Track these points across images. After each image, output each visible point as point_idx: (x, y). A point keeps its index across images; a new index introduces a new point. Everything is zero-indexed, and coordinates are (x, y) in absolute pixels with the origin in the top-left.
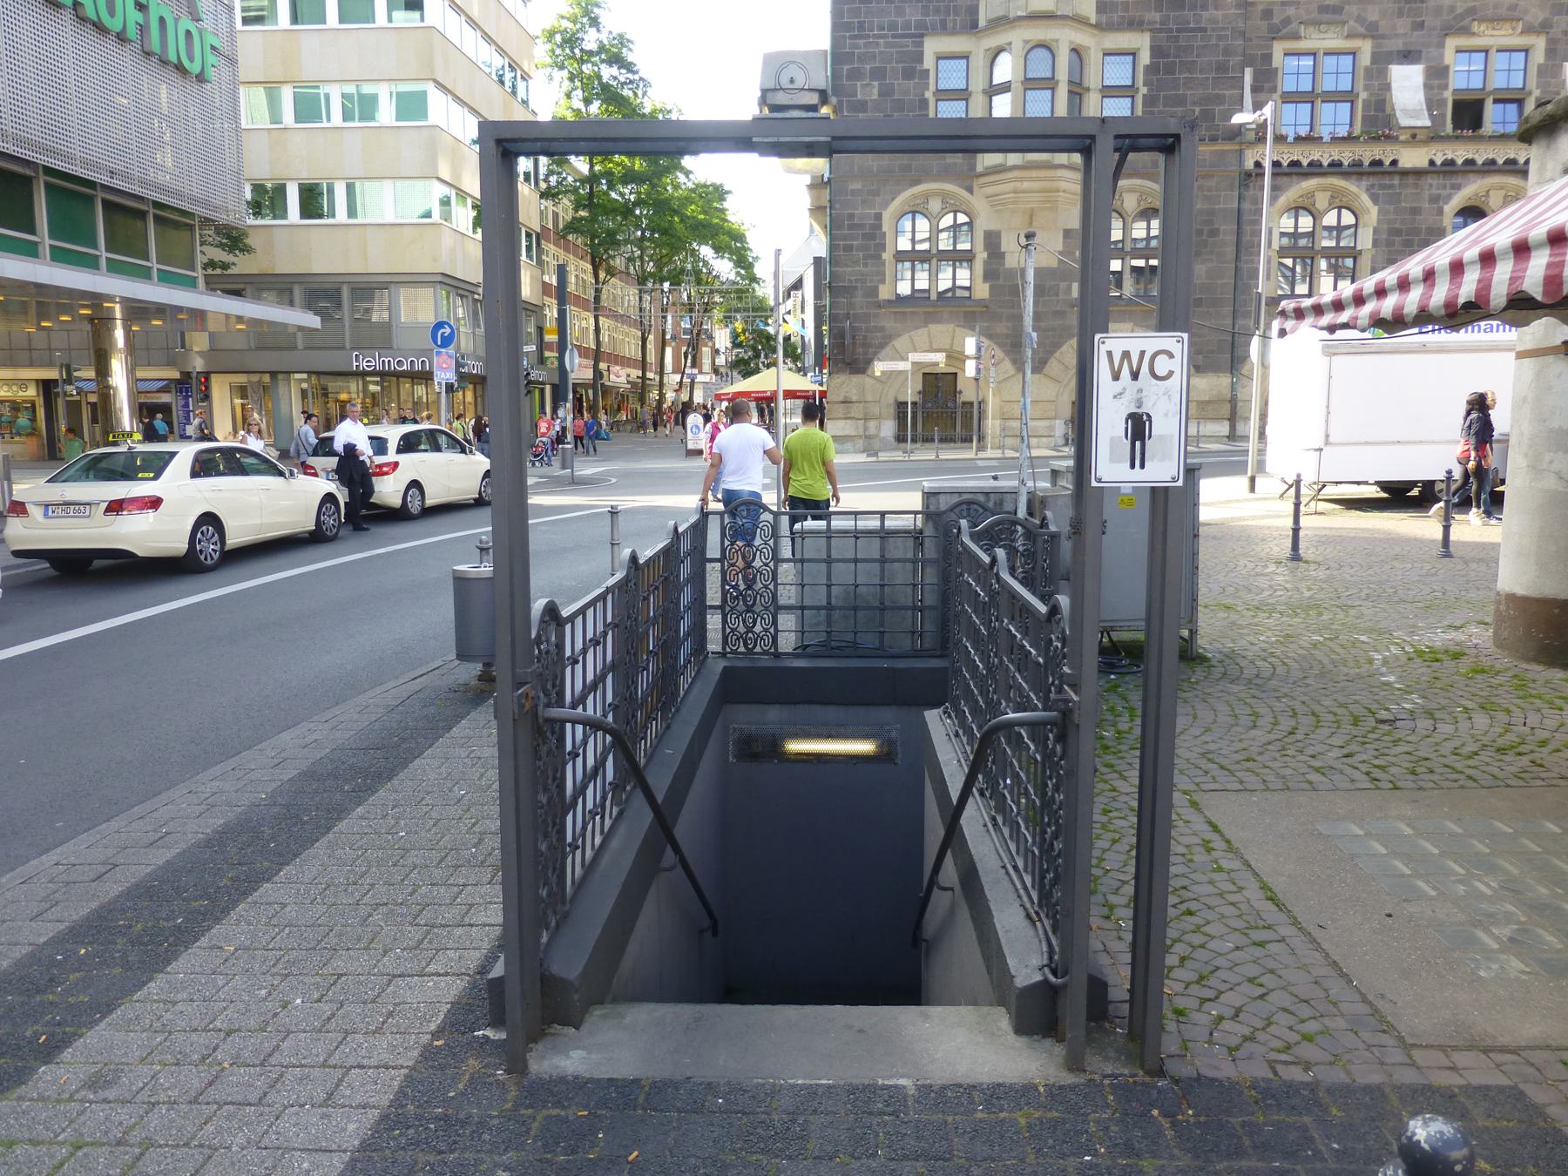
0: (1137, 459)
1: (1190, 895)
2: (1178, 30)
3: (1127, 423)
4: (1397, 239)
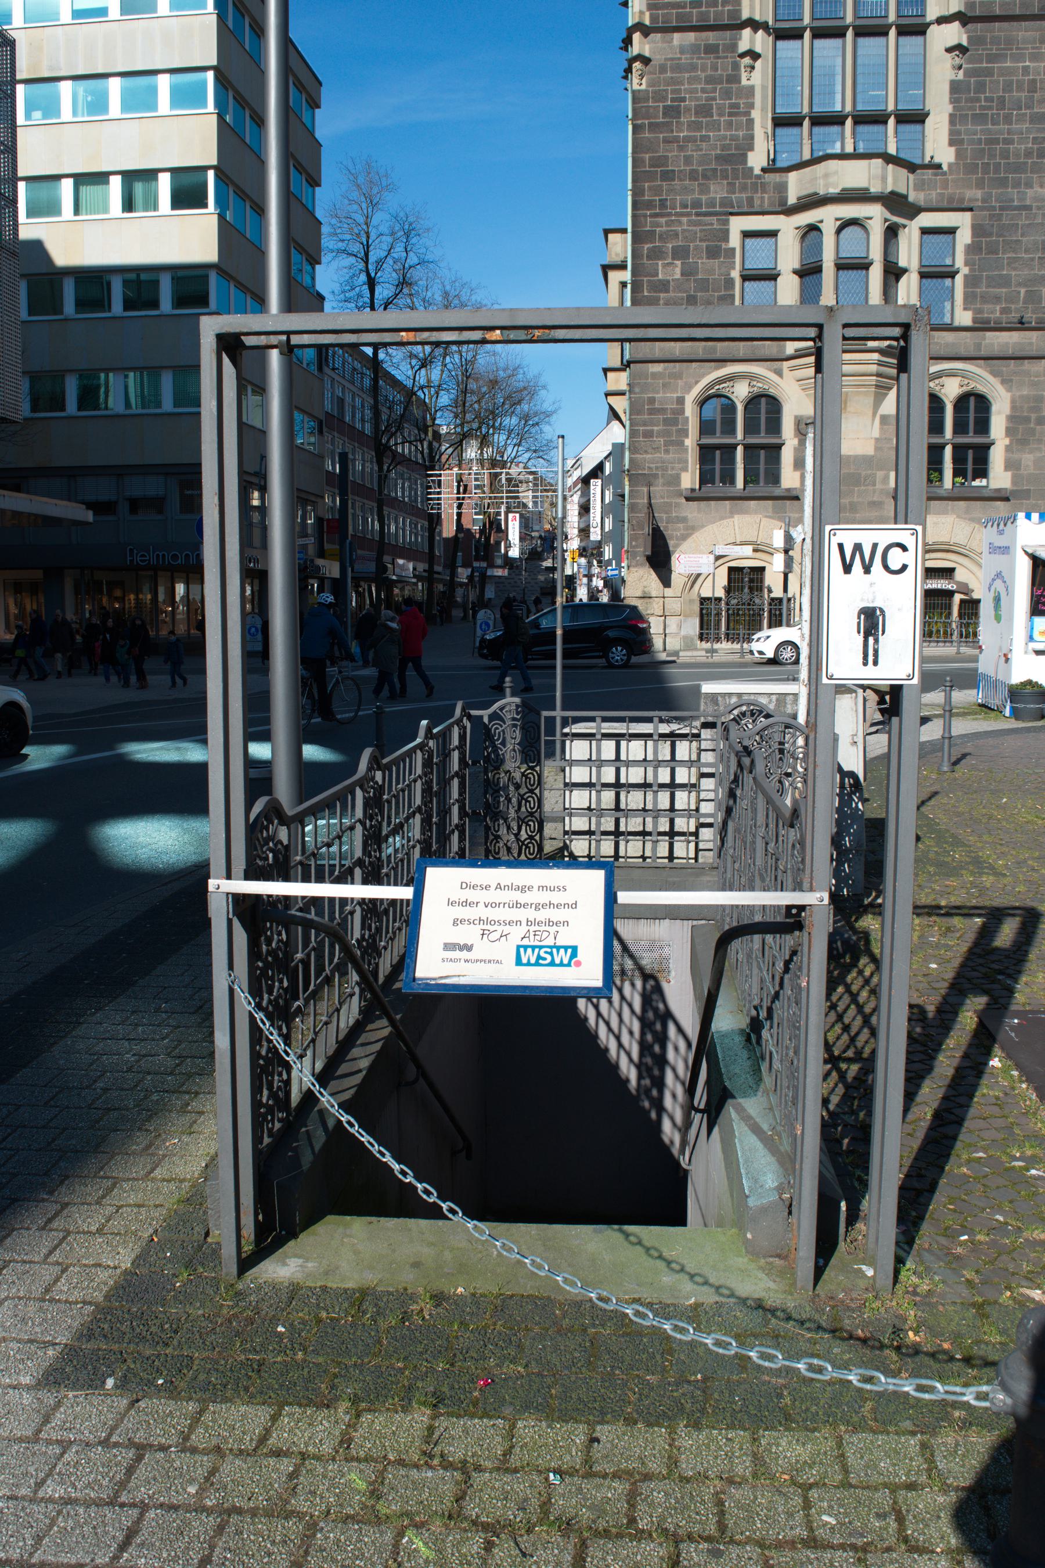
0: (870, 656)
1: (952, 1117)
2: (1002, 208)
3: (859, 618)
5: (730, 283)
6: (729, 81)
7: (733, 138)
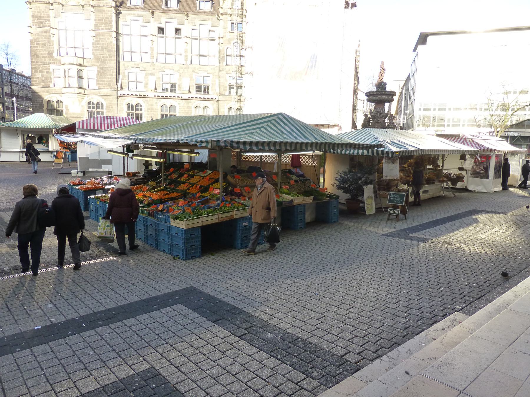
4: (149, 111)
5: (51, 78)
6: (49, 39)
7: (50, 50)
